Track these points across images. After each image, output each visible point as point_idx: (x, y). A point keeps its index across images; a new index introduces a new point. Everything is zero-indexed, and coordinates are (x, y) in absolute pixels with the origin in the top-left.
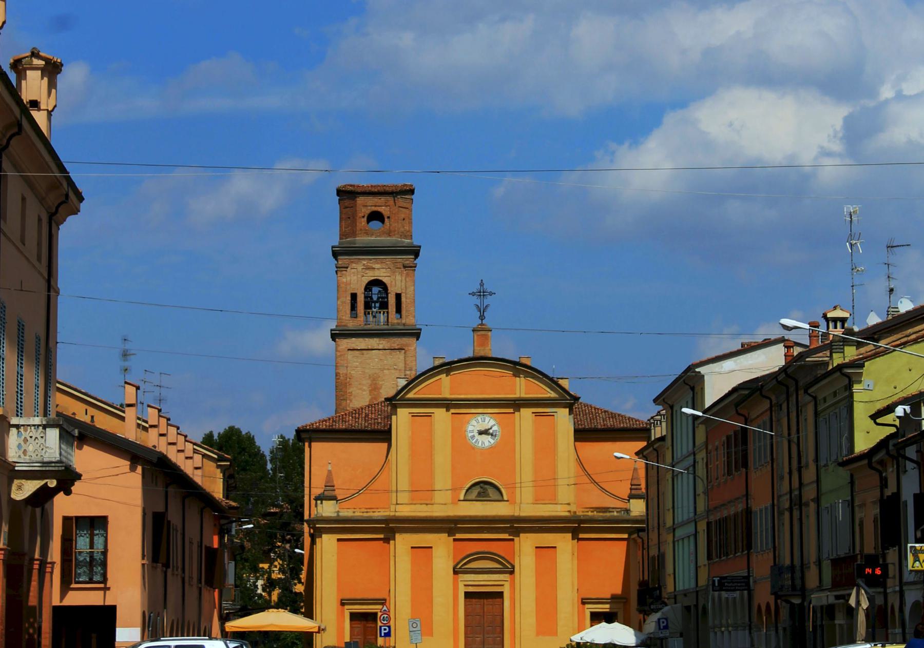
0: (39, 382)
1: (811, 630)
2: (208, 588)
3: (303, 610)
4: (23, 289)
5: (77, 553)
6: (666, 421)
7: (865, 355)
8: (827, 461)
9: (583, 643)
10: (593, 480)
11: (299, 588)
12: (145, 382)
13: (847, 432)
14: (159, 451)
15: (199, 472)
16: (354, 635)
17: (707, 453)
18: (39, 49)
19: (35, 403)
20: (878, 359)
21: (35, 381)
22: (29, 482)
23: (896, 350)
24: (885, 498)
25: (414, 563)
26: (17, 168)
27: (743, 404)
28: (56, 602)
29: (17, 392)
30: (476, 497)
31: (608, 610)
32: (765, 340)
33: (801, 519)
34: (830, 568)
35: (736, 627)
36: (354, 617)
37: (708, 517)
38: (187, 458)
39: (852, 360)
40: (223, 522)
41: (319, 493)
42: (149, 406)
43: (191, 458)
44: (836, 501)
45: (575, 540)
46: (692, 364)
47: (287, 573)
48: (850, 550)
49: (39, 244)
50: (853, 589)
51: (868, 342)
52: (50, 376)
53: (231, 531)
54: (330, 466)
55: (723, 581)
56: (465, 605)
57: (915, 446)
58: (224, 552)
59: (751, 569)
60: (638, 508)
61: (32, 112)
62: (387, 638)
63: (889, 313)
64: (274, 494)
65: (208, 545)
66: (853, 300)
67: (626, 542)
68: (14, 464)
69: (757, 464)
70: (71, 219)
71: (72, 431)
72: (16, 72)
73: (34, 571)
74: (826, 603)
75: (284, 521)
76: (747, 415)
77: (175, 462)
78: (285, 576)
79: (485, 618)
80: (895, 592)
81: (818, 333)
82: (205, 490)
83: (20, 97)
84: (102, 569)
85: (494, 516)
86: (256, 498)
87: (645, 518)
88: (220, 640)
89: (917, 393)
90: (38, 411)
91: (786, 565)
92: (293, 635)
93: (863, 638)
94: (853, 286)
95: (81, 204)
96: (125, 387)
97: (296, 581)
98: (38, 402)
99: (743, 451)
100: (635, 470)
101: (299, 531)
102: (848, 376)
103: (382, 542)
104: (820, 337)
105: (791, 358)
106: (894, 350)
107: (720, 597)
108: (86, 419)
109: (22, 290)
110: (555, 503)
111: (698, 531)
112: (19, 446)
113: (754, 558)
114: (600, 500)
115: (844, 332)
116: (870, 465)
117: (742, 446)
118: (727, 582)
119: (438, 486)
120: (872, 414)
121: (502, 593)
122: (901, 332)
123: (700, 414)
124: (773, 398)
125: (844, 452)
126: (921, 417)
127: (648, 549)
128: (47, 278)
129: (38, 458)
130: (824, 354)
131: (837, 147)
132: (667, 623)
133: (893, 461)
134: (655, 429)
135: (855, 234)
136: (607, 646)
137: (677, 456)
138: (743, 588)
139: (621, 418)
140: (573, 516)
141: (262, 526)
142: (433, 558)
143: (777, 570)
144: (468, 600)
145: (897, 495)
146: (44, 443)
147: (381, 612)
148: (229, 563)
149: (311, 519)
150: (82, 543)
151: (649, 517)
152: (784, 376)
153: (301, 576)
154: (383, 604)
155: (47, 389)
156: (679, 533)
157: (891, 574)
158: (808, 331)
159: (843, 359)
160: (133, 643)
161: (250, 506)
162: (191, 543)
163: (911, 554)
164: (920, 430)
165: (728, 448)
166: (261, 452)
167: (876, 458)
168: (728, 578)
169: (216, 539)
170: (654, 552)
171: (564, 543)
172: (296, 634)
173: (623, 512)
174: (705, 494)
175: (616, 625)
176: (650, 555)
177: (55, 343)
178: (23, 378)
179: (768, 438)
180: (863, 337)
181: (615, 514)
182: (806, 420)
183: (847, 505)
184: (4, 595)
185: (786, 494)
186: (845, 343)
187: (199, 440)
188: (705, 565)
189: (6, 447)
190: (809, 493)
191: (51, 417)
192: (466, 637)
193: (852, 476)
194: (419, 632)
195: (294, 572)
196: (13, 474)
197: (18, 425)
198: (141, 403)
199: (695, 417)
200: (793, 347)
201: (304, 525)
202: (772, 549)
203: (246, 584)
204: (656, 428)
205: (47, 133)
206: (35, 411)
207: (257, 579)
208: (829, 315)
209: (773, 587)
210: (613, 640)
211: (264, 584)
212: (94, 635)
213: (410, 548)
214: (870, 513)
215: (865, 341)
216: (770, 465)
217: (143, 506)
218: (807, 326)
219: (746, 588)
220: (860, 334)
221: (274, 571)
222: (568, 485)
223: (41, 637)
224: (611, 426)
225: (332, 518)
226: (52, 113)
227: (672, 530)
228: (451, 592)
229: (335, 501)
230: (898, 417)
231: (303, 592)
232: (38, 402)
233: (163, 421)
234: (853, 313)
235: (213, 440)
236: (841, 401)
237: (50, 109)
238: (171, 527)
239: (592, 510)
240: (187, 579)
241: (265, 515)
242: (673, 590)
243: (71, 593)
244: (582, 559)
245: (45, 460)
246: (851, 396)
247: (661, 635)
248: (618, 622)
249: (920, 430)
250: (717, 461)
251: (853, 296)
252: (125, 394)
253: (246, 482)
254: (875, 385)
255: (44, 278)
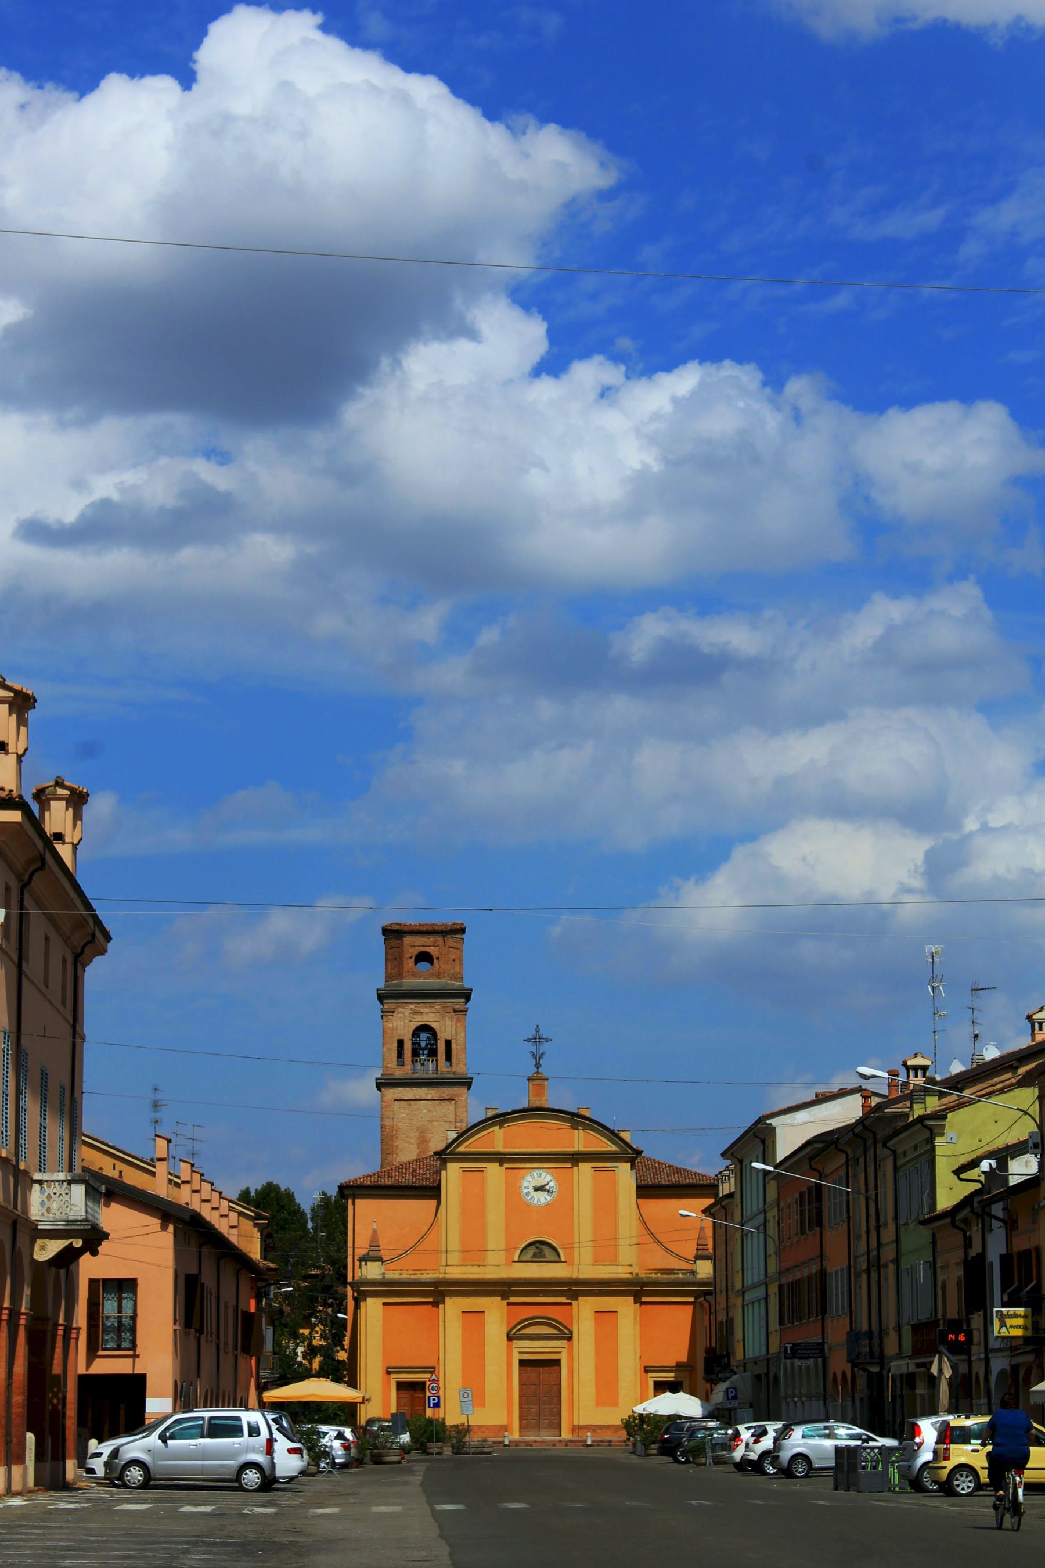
0: (63, 1135)
1: (890, 1400)
2: (245, 1355)
3: (346, 1379)
4: (47, 1035)
5: (105, 1318)
6: (735, 1177)
7: (948, 1106)
8: (907, 1219)
9: (646, 1414)
10: (657, 1240)
11: (342, 1356)
12: (177, 1134)
13: (928, 1189)
14: (192, 1208)
15: (234, 1231)
16: (400, 1406)
17: (778, 1211)
18: (63, 777)
19: (59, 1158)
20: (961, 1110)
21: (59, 1134)
22: (53, 1241)
23: (980, 1101)
24: (970, 1258)
25: (465, 1328)
26: (40, 905)
27: (817, 1159)
28: (82, 1370)
29: (40, 1145)
30: (531, 1258)
31: (672, 1379)
32: (841, 1089)
33: (879, 1282)
34: (911, 1334)
35: (810, 1397)
36: (401, 1386)
37: (779, 1280)
38: (222, 1216)
39: (935, 1111)
40: (260, 1284)
41: (364, 1254)
42: (181, 1160)
43: (226, 1216)
44: (917, 1262)
45: (637, 1303)
46: (763, 1116)
47: (329, 1339)
48: (931, 1315)
49: (64, 987)
50: (935, 1356)
51: (951, 1092)
52: (76, 1128)
53: (269, 1294)
54: (375, 1224)
55: (796, 1348)
56: (520, 1374)
57: (1001, 1203)
58: (262, 1317)
59: (826, 1335)
60: (705, 1269)
61: (56, 846)
62: (436, 1409)
63: (974, 1061)
64: (315, 1255)
65: (244, 1310)
66: (935, 1047)
67: (692, 1306)
68: (37, 1223)
69: (833, 1223)
70: (97, 960)
71: (99, 1187)
72: (39, 803)
73: (58, 1337)
74: (907, 1372)
75: (326, 1284)
76: (821, 1171)
77: (209, 1220)
78: (327, 1342)
79: (541, 1388)
80: (980, 1359)
81: (898, 1082)
82: (241, 1250)
83: (43, 830)
84: (131, 1335)
85: (551, 1279)
86: (296, 1259)
87: (712, 1280)
88: (258, 1411)
89: (1003, 1146)
90: (63, 1166)
91: (864, 1331)
92: (336, 1406)
93: (946, 1409)
94: (935, 1032)
95: (109, 944)
96: (155, 1140)
97: (339, 1348)
98: (62, 1156)
99: (817, 1208)
100: (702, 1229)
101: (342, 1295)
102: (930, 1128)
103: (430, 1306)
104: (900, 1087)
105: (869, 1109)
106: (979, 1101)
107: (792, 1365)
108: (115, 1174)
109: (45, 1036)
110: (616, 1264)
111: (769, 1294)
112: (42, 1203)
113: (829, 1323)
114: (663, 1260)
115: (925, 1081)
116: (953, 1224)
117: (816, 1204)
118: (800, 1349)
119: (490, 1246)
120: (955, 1168)
121: (559, 1360)
122: (987, 1081)
123: (771, 1169)
124: (850, 1152)
125: (926, 1210)
126: (1008, 1172)
127: (716, 1313)
128: (72, 1023)
129: (63, 1217)
130: (904, 1104)
131: (918, 883)
132: (736, 1393)
133: (978, 1220)
134: (723, 1185)
135: (937, 976)
136: (672, 1417)
137: (746, 1213)
138: (818, 1355)
139: (686, 1173)
140: (635, 1278)
141: (302, 1289)
142: (486, 1324)
143: (854, 1336)
144: (522, 1368)
145: (982, 1256)
146: (69, 1200)
147: (429, 1381)
148: (266, 1329)
149: (355, 1281)
150: (109, 1307)
151: (717, 1279)
152: (861, 1128)
153: (344, 1343)
154: (432, 1373)
155: (72, 1142)
156: (748, 1296)
157: (975, 1340)
158: (887, 1080)
159: (924, 1110)
160: (165, 1415)
161: (290, 1268)
162: (226, 1307)
163: (997, 1319)
164: (1007, 1187)
165: (801, 1206)
166: (302, 1210)
167: (960, 1216)
168: (801, 1345)
169: (253, 1303)
170: (722, 1317)
171: (625, 1307)
172: (339, 1404)
173: (688, 1274)
174: (777, 1254)
175: (681, 1395)
176: (718, 1320)
177: (81, 1093)
178: (47, 1130)
179: (844, 1194)
180: (946, 1086)
181: (680, 1276)
182: (884, 1175)
183: (928, 1266)
184: (26, 1363)
185: (863, 1255)
186: (927, 1093)
187: (235, 1198)
188: (776, 1331)
189: (28, 1203)
190: (888, 1253)
191: (76, 1172)
192: (521, 1408)
193: (934, 1235)
194: (471, 1402)
195: (337, 1338)
196: (37, 1233)
197: (41, 1181)
198: (172, 1157)
199: (766, 1173)
200: (870, 1097)
201: (346, 1287)
202: (848, 1314)
203: (285, 1352)
204: (724, 1184)
205: (72, 867)
206: (59, 1165)
207: (297, 1346)
208: (909, 1063)
209: (849, 1354)
210: (678, 1411)
211: (305, 1351)
212: (122, 1406)
213: (461, 1312)
214: (953, 1275)
215: (948, 1091)
216: (846, 1223)
217: (175, 1267)
218: (886, 1075)
219: (821, 1355)
220: (945, 1083)
221: (315, 1337)
222: (630, 1245)
223: (66, 1409)
224: (676, 1181)
225: (377, 1281)
226: (78, 847)
227: (741, 1294)
228: (505, 1359)
229: (381, 1263)
230: (983, 1172)
231: (346, 1360)
232: (62, 1156)
233: (197, 1176)
234: (935, 1061)
235: (250, 1197)
236: (922, 1155)
237: (75, 843)
238: (205, 1291)
239: (655, 1272)
240: (222, 1346)
241: (306, 1277)
242: (742, 1358)
243: (97, 1361)
244: (645, 1325)
245: (70, 1218)
246: (933, 1149)
247: (730, 1406)
248: (683, 1392)
249: (1007, 1187)
250: (790, 1219)
251: (935, 1043)
252: (155, 1148)
253: (285, 1242)
254: (959, 1137)
255: (68, 1023)
